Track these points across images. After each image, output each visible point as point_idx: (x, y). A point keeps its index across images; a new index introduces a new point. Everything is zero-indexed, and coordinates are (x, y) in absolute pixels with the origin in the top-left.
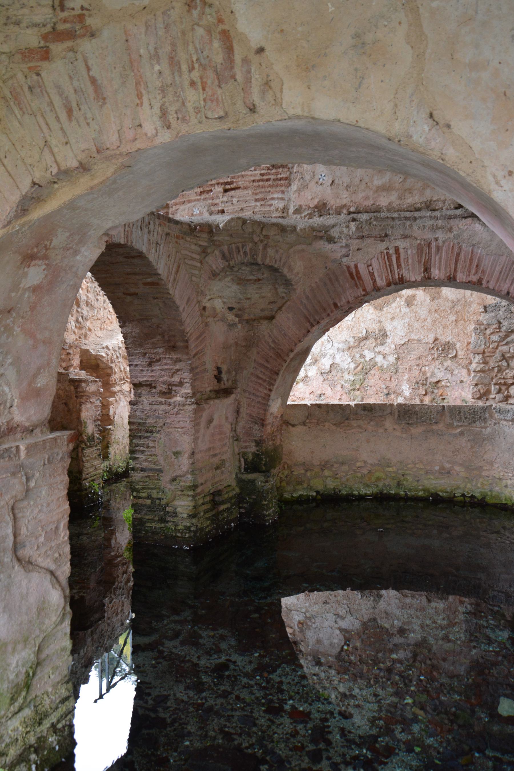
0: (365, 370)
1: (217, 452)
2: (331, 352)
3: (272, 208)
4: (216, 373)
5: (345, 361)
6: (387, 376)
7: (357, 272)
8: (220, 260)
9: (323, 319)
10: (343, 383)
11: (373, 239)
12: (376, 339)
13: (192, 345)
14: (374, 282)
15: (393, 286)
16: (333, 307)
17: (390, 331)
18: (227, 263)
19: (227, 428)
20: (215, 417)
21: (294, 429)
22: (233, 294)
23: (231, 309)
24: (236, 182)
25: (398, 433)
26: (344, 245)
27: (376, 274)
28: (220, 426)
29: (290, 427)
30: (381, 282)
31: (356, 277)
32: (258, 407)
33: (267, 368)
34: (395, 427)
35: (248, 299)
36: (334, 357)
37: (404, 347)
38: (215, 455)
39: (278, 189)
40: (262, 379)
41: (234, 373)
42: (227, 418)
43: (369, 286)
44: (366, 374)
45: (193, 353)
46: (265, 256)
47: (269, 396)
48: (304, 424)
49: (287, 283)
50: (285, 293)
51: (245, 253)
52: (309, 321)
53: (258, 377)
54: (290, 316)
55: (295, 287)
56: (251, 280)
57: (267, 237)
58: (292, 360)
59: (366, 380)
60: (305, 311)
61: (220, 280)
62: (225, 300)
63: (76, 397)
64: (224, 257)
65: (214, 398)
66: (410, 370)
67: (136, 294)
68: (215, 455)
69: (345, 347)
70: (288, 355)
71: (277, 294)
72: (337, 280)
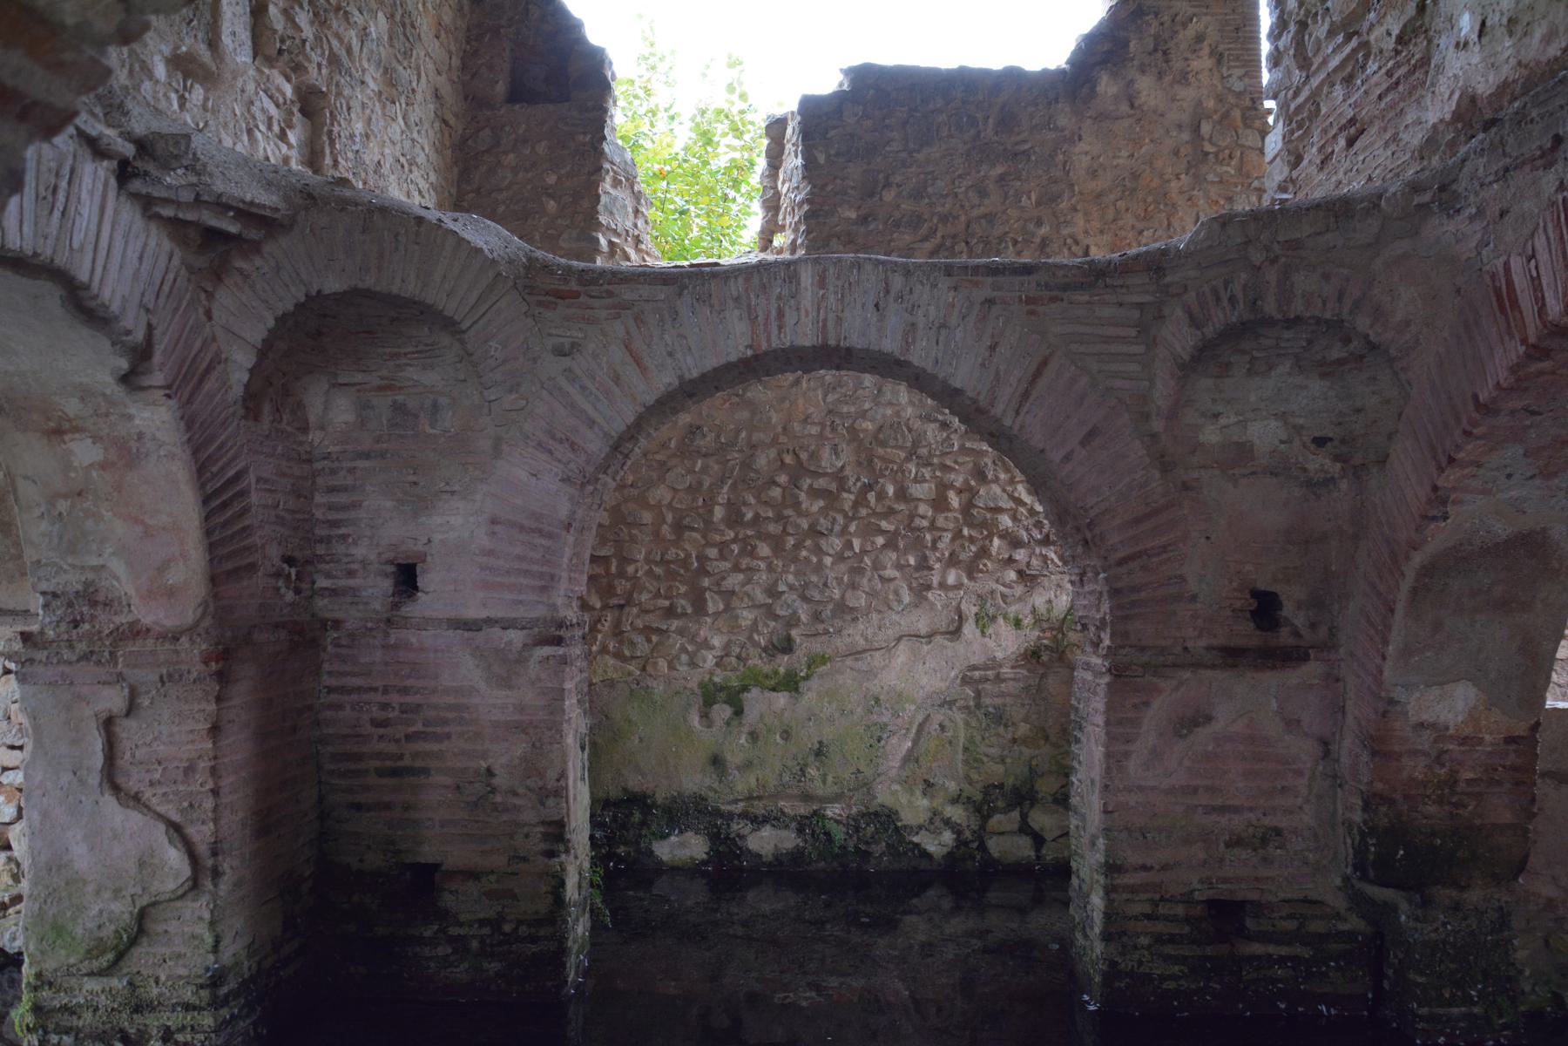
7: (1510, 283)
11: (1527, 168)
35: (1359, 411)
42: (1292, 724)
51: (1232, 300)
57: (1294, 245)
62: (1301, 421)
65: (1213, 667)
70: (1408, 558)
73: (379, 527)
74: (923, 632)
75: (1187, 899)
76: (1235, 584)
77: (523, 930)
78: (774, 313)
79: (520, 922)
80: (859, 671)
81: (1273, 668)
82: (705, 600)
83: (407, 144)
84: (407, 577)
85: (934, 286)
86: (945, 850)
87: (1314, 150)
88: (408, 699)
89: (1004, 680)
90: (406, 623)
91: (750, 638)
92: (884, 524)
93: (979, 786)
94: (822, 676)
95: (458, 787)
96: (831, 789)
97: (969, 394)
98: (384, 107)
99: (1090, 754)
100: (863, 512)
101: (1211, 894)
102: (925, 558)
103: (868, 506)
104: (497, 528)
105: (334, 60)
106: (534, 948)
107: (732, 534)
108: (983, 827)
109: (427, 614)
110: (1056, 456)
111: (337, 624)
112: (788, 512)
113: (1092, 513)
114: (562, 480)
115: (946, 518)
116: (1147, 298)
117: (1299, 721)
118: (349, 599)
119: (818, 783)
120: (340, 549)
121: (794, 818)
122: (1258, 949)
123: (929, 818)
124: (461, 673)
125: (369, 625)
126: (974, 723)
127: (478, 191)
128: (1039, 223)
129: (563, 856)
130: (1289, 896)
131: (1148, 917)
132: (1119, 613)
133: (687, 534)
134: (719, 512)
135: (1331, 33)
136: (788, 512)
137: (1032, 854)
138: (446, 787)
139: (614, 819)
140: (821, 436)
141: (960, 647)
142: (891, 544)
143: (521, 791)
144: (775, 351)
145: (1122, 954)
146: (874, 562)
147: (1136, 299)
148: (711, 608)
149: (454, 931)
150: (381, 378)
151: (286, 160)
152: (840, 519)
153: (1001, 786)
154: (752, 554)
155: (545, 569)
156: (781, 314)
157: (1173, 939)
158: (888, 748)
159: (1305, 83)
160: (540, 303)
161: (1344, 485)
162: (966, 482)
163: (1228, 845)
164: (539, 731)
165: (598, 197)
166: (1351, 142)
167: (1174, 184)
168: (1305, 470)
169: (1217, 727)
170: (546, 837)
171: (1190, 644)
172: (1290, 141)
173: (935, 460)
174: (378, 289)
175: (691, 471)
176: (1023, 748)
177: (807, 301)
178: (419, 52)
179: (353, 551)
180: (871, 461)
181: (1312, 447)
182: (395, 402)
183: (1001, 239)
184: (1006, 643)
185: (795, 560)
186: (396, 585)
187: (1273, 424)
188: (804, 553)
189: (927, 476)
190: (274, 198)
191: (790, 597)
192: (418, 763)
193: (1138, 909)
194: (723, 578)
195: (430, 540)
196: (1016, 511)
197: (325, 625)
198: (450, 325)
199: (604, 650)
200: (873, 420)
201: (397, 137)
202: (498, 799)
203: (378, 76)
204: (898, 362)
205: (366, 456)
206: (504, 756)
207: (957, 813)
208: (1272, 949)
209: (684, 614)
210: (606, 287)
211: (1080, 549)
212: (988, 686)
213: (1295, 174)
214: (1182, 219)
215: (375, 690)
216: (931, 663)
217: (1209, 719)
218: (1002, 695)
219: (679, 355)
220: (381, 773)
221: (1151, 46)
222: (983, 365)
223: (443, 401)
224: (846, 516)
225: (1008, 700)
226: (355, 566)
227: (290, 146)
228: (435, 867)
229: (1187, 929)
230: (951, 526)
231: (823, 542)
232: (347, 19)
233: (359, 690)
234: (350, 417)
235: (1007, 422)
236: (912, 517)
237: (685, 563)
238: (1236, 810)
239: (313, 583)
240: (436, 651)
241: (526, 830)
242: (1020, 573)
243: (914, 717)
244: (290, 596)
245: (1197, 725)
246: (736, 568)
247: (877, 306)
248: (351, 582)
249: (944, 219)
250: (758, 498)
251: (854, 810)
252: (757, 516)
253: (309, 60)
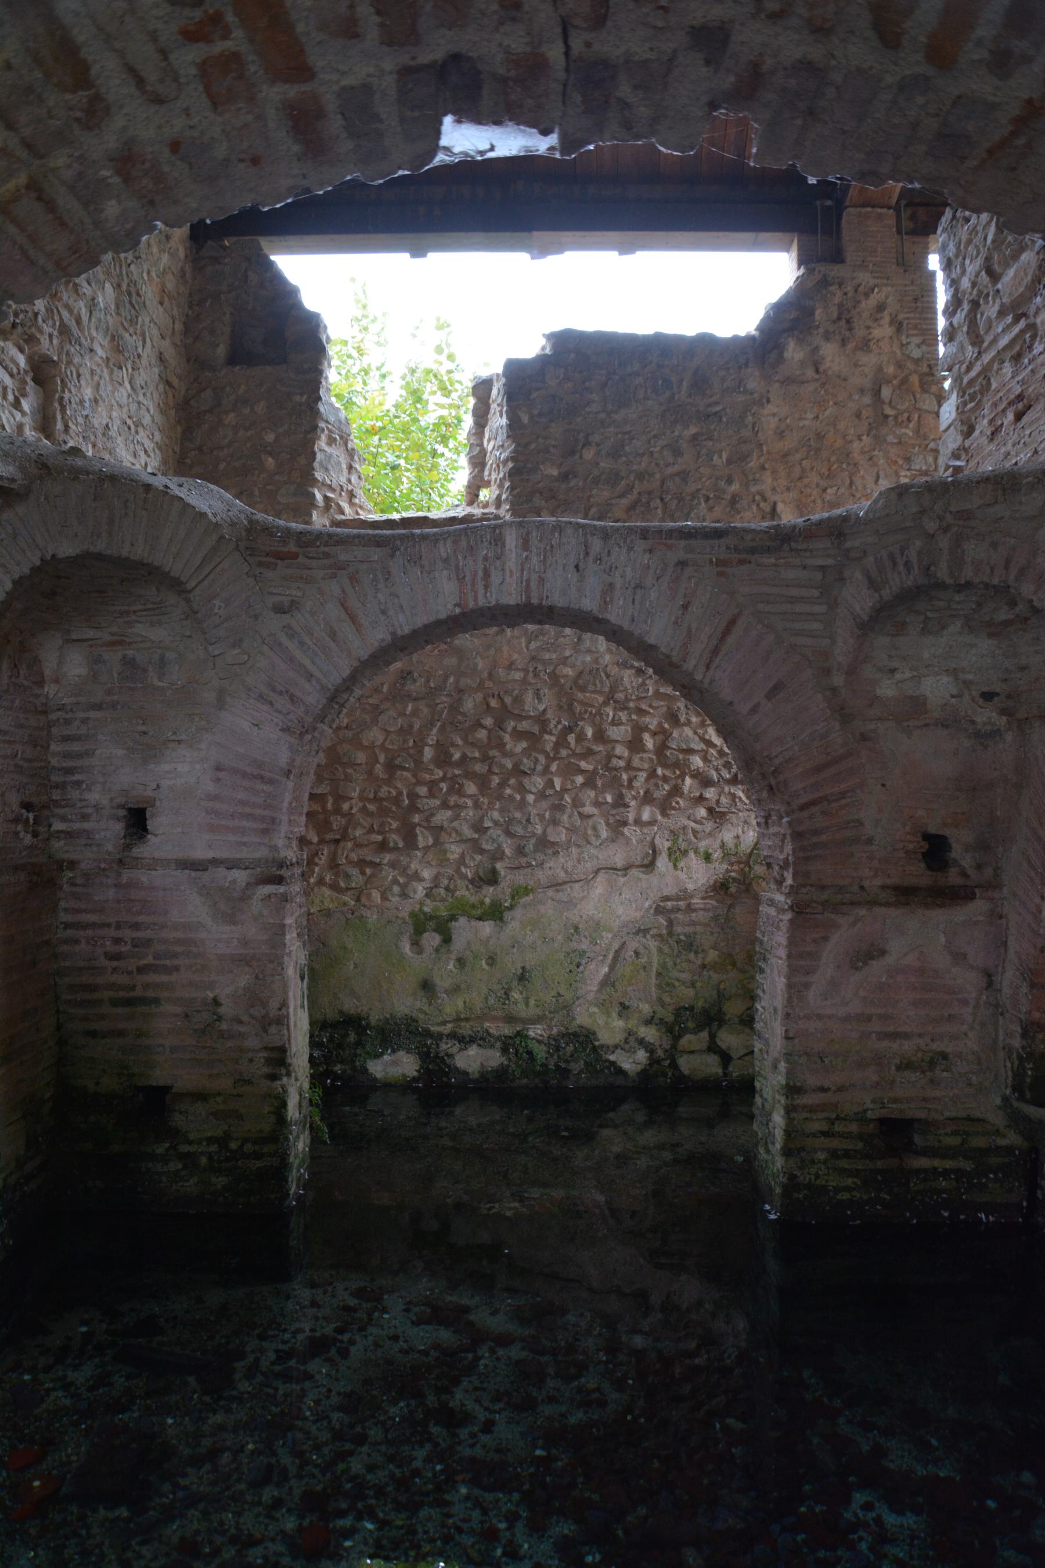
18: (876, 595)
23: (988, 696)
35: (1023, 668)
42: (958, 957)
51: (907, 564)
53: (1029, 862)
57: (965, 516)
62: (970, 677)
65: (887, 904)
73: (112, 773)
74: (619, 865)
75: (861, 1118)
76: (908, 829)
77: (249, 1147)
78: (480, 574)
79: (245, 1140)
80: (559, 902)
81: (941, 906)
82: (416, 835)
83: (134, 407)
84: (138, 821)
85: (631, 549)
86: (639, 1068)
87: (985, 421)
88: (140, 934)
89: (695, 910)
90: (137, 863)
91: (458, 871)
92: (583, 764)
93: (671, 1008)
94: (525, 906)
95: (187, 1016)
96: (533, 1011)
97: (663, 650)
98: (111, 373)
99: (773, 984)
100: (564, 753)
101: (884, 1113)
102: (621, 796)
103: (568, 747)
104: (221, 775)
105: (64, 330)
106: (259, 1164)
107: (441, 774)
108: (674, 1046)
109: (156, 855)
110: (744, 708)
111: (72, 864)
112: (493, 753)
113: (777, 762)
114: (282, 730)
115: (641, 759)
116: (830, 562)
117: (965, 955)
118: (83, 841)
119: (521, 1006)
120: (74, 794)
121: (499, 1038)
122: (923, 1162)
123: (623, 1036)
124: (189, 911)
125: (103, 866)
126: (666, 949)
127: (200, 449)
128: (730, 481)
129: (285, 1079)
130: (954, 1114)
131: (825, 1134)
132: (801, 855)
133: (399, 773)
134: (428, 753)
135: (1001, 314)
136: (493, 753)
137: (720, 1071)
138: (175, 1015)
139: (331, 1039)
140: (524, 681)
141: (654, 879)
142: (590, 783)
143: (245, 1018)
144: (481, 609)
145: (801, 1168)
146: (573, 800)
147: (820, 562)
148: (421, 842)
149: (185, 1148)
150: (112, 634)
151: (20, 427)
152: (542, 759)
153: (691, 1008)
154: (460, 792)
155: (266, 813)
156: (487, 574)
157: (847, 1154)
158: (587, 973)
159: (977, 359)
160: (260, 564)
161: (1009, 737)
162: (660, 724)
163: (899, 1068)
164: (264, 962)
165: (314, 454)
166: (1019, 416)
167: (856, 445)
168: (973, 722)
169: (890, 960)
170: (269, 1061)
171: (866, 884)
172: (963, 412)
173: (632, 705)
174: (109, 552)
175: (403, 714)
176: (711, 973)
177: (512, 562)
178: (144, 319)
179: (87, 796)
180: (570, 706)
181: (981, 701)
182: (124, 657)
183: (694, 495)
184: (697, 875)
185: (500, 797)
186: (127, 828)
187: (945, 679)
188: (508, 791)
189: (624, 719)
190: (11, 468)
191: (496, 832)
192: (150, 994)
193: (816, 1127)
194: (432, 815)
195: (158, 786)
196: (706, 752)
197: (61, 865)
198: (177, 585)
199: (321, 882)
200: (573, 666)
201: (124, 400)
202: (224, 1026)
203: (105, 343)
204: (597, 620)
205: (99, 707)
206: (229, 988)
207: (650, 1034)
208: (937, 1163)
209: (396, 849)
210: (323, 549)
211: (765, 794)
212: (680, 916)
213: (967, 443)
214: (863, 477)
215: (109, 925)
216: (626, 895)
217: (883, 953)
218: (694, 924)
219: (391, 613)
220: (115, 1003)
221: (835, 315)
222: (676, 623)
223: (170, 655)
224: (547, 756)
225: (699, 929)
226: (89, 810)
227: (23, 413)
228: (166, 1089)
229: (860, 1145)
230: (646, 766)
231: (526, 781)
232: (76, 292)
233: (93, 925)
234: (83, 671)
235: (698, 677)
236: (610, 756)
237: (397, 800)
238: (906, 1036)
239: (50, 826)
240: (165, 889)
241: (250, 1055)
242: (710, 810)
243: (610, 944)
244: (28, 839)
245: (872, 958)
246: (445, 805)
247: (577, 567)
248: (86, 826)
249: (641, 476)
250: (465, 740)
251: (555, 1031)
252: (464, 757)
253: (41, 332)
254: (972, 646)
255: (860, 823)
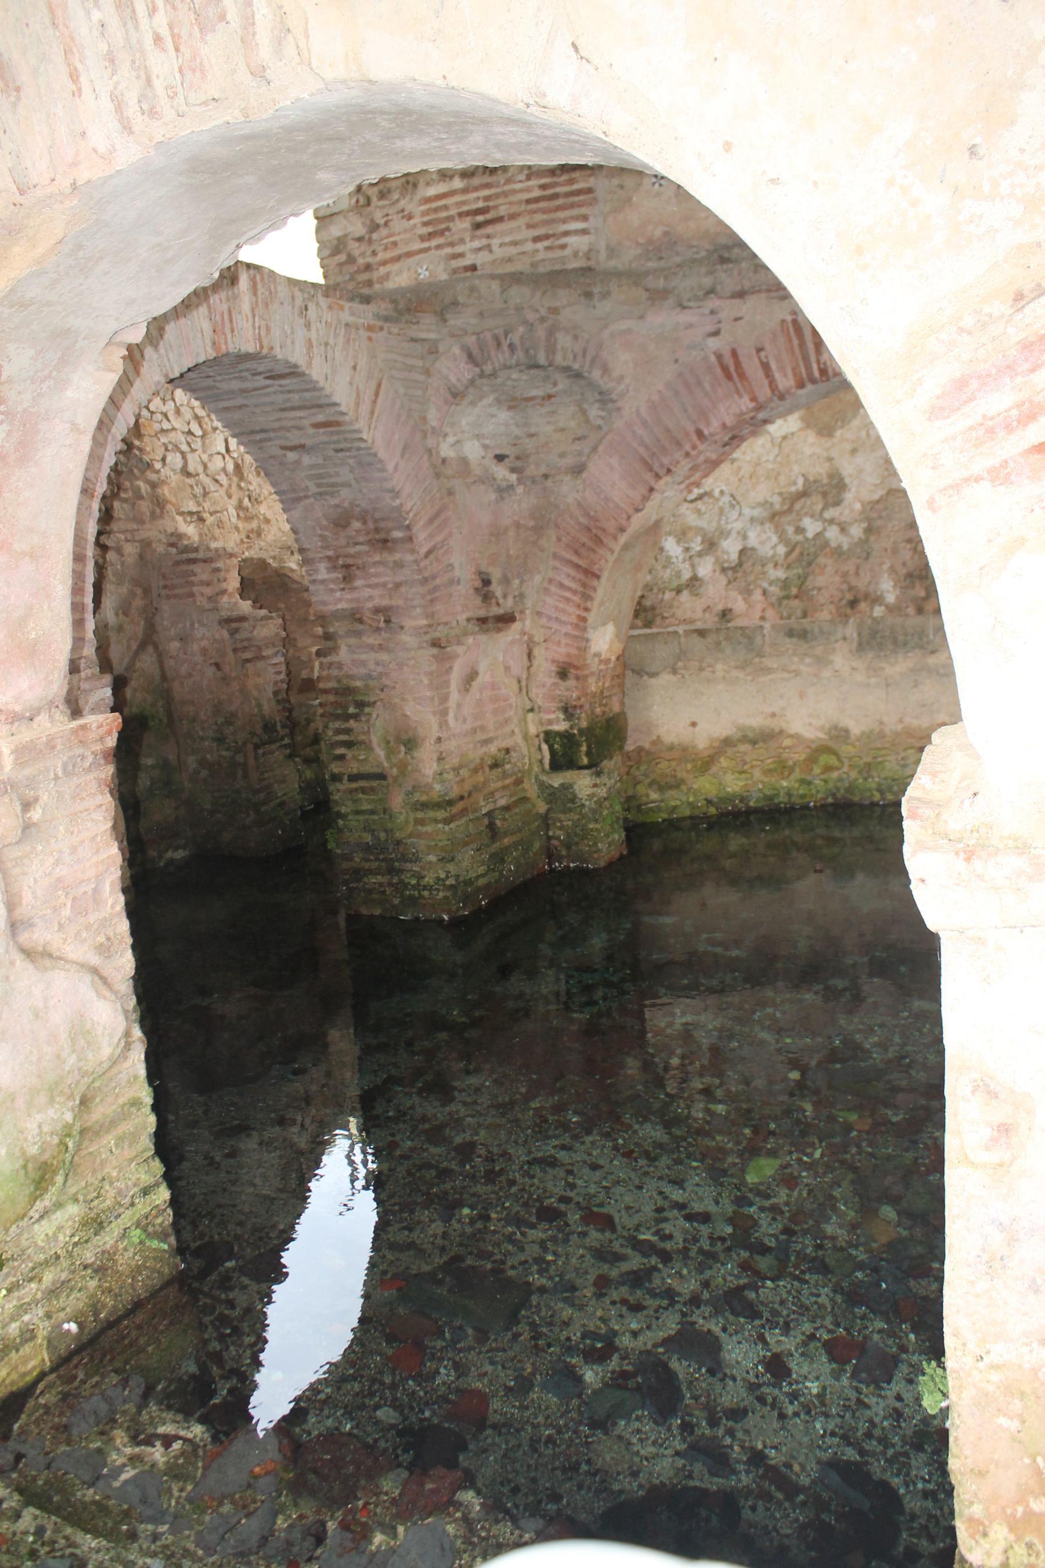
0: (805, 557)
1: (491, 735)
2: (738, 526)
3: (567, 252)
4: (478, 583)
5: (766, 542)
6: (850, 567)
7: (738, 364)
8: (462, 365)
9: (678, 462)
10: (765, 585)
11: (763, 295)
12: (824, 494)
13: (421, 535)
14: (772, 383)
15: (809, 387)
16: (694, 438)
17: (850, 476)
18: (477, 370)
19: (509, 689)
20: (482, 668)
21: (653, 681)
22: (503, 428)
23: (500, 458)
24: (495, 207)
25: (860, 677)
26: (707, 312)
27: (773, 366)
28: (494, 686)
29: (646, 677)
30: (785, 381)
31: (735, 375)
32: (567, 645)
33: (577, 566)
34: (855, 664)
35: (532, 435)
36: (745, 537)
37: (880, 506)
38: (487, 742)
39: (576, 212)
40: (569, 589)
41: (517, 581)
42: (507, 669)
43: (764, 392)
44: (810, 564)
45: (424, 550)
46: (551, 349)
47: (584, 620)
48: (674, 671)
49: (605, 399)
50: (603, 418)
51: (511, 346)
52: (651, 470)
53: (562, 586)
54: (614, 461)
55: (619, 404)
56: (533, 398)
58: (626, 547)
59: (811, 578)
60: (642, 451)
61: (473, 403)
62: (487, 442)
63: (235, 650)
64: (471, 357)
66: (895, 551)
67: (302, 447)
68: (487, 742)
69: (765, 514)
70: (615, 538)
71: (587, 421)
72: (699, 383)
161: (520, 490)
254: (493, 416)
255: (451, 566)
